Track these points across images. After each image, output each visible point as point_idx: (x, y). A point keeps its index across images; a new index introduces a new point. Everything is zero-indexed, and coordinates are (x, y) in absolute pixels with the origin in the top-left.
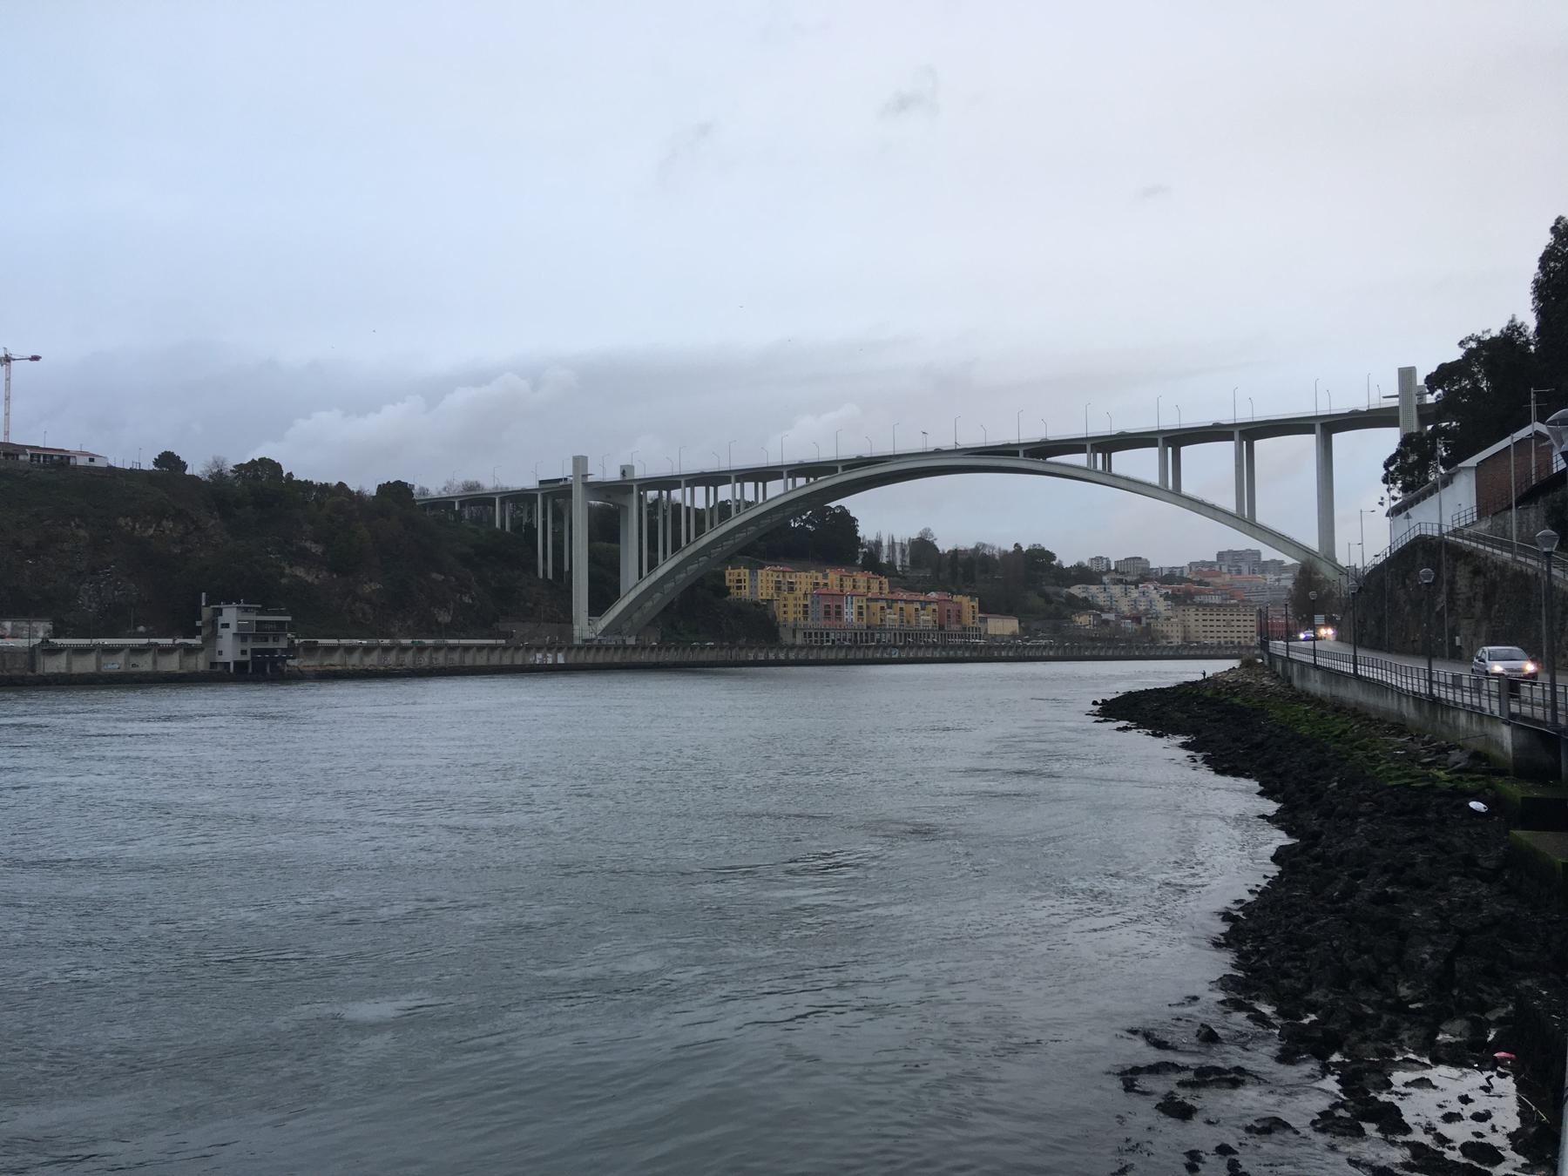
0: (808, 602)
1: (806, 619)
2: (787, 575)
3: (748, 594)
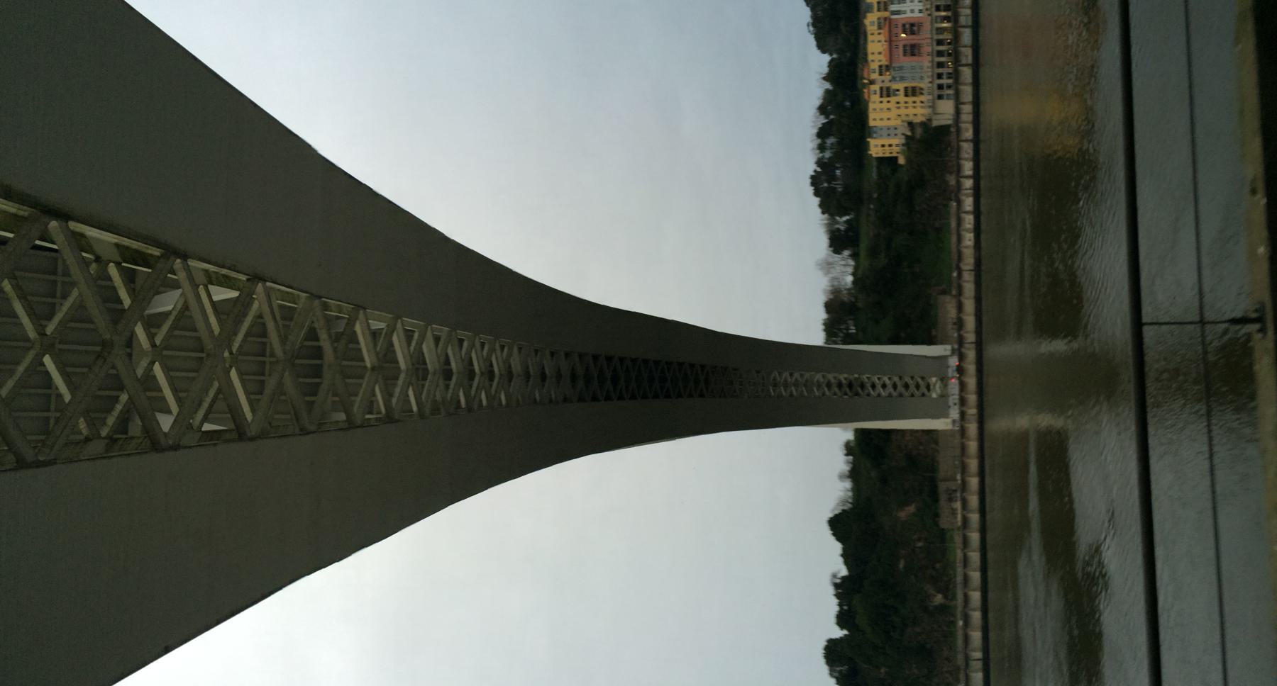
3: (895, 141)
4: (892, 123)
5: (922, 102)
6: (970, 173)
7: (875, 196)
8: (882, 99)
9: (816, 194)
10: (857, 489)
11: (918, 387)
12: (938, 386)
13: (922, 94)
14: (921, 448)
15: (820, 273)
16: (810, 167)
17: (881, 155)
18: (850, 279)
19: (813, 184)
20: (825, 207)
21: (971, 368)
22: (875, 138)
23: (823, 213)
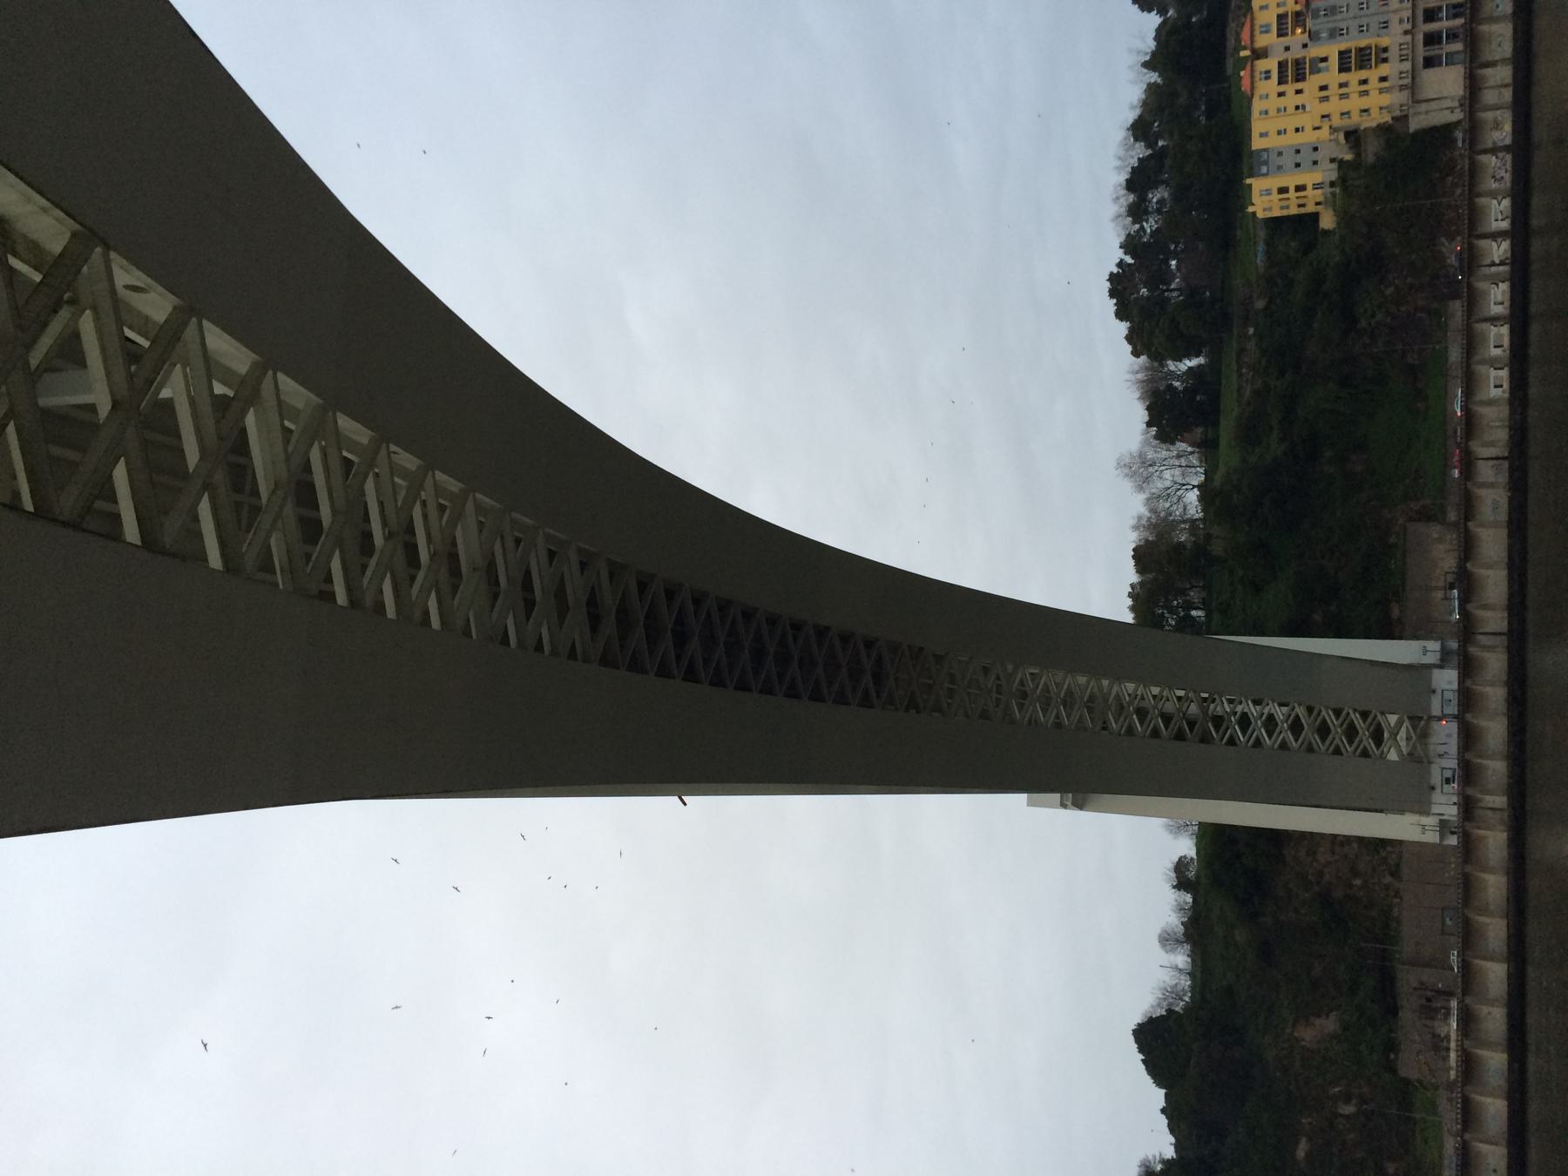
0: (1332, 50)
1: (1382, 55)
2: (1262, 41)
3: (1317, 177)
4: (1309, 137)
5: (1383, 79)
6: (1505, 225)
7: (1260, 304)
8: (1282, 88)
9: (1121, 314)
10: (1201, 971)
11: (1351, 732)
12: (1402, 734)
13: (1385, 60)
14: (1358, 882)
15: (1127, 485)
16: (1111, 255)
17: (1277, 213)
18: (1192, 497)
19: (1112, 294)
20: (1139, 341)
21: (1495, 695)
22: (1264, 175)
23: (1136, 353)
